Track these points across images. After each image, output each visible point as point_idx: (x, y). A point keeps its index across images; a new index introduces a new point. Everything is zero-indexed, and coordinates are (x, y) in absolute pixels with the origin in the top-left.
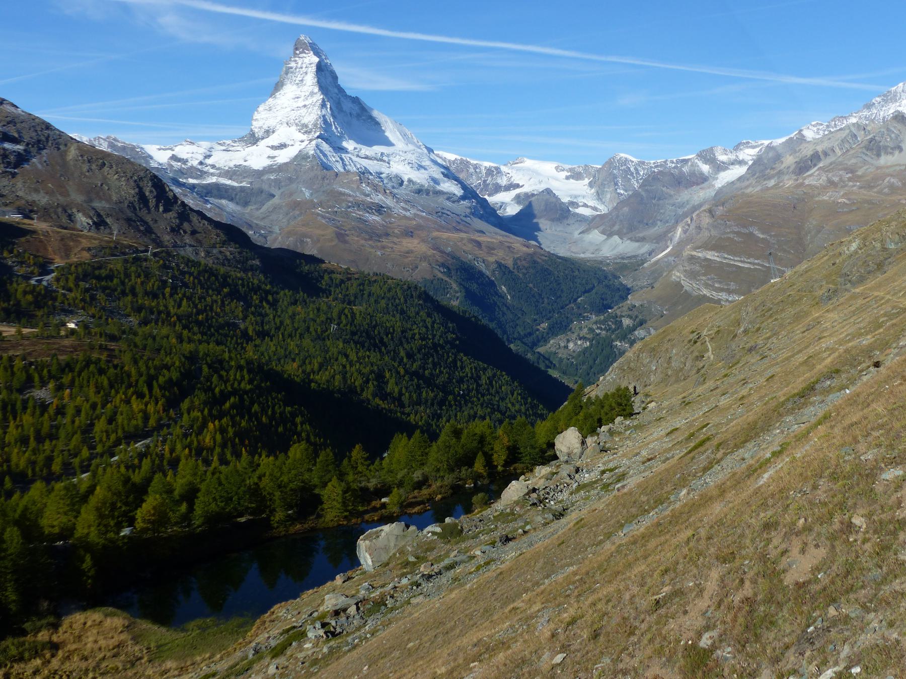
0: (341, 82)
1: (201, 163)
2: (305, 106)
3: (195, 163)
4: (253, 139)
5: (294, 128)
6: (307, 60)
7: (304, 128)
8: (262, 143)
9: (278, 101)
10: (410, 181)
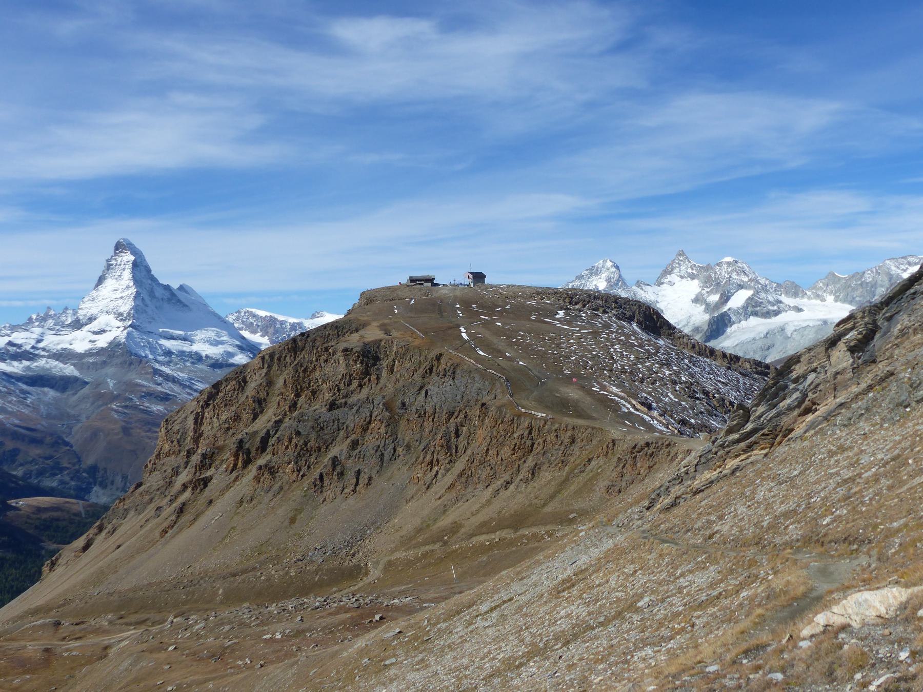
0: (154, 272)
1: (33, 347)
2: (122, 297)
3: (28, 347)
4: (77, 325)
5: (112, 316)
6: (125, 259)
7: (120, 316)
8: (86, 328)
9: (101, 293)
10: (207, 357)
